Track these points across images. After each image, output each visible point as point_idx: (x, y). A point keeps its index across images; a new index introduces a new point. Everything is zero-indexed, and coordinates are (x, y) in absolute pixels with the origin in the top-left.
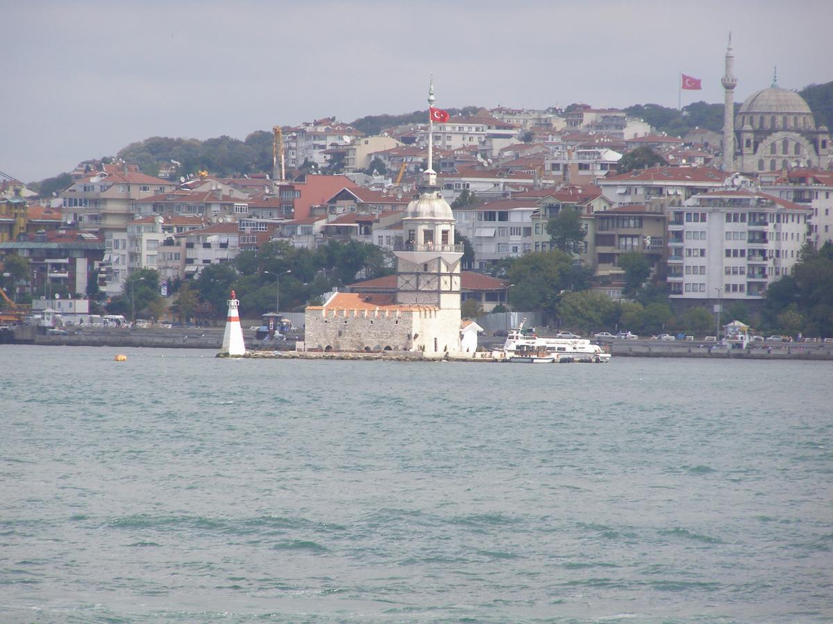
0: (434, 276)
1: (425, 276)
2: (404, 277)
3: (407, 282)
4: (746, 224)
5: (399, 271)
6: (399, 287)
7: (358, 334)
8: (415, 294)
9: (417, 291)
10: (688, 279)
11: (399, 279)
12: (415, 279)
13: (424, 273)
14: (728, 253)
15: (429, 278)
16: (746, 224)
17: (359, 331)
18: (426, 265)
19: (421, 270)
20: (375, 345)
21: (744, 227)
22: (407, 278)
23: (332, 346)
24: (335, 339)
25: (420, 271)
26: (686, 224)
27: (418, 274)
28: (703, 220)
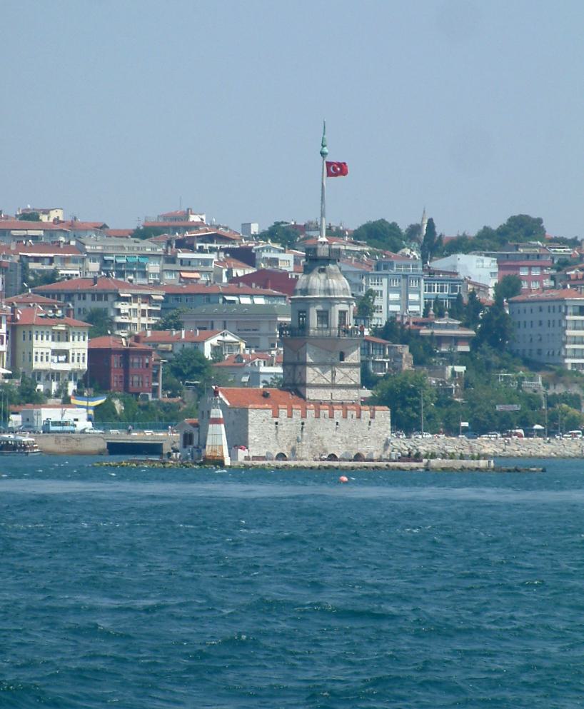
15: (346, 370)
17: (321, 435)
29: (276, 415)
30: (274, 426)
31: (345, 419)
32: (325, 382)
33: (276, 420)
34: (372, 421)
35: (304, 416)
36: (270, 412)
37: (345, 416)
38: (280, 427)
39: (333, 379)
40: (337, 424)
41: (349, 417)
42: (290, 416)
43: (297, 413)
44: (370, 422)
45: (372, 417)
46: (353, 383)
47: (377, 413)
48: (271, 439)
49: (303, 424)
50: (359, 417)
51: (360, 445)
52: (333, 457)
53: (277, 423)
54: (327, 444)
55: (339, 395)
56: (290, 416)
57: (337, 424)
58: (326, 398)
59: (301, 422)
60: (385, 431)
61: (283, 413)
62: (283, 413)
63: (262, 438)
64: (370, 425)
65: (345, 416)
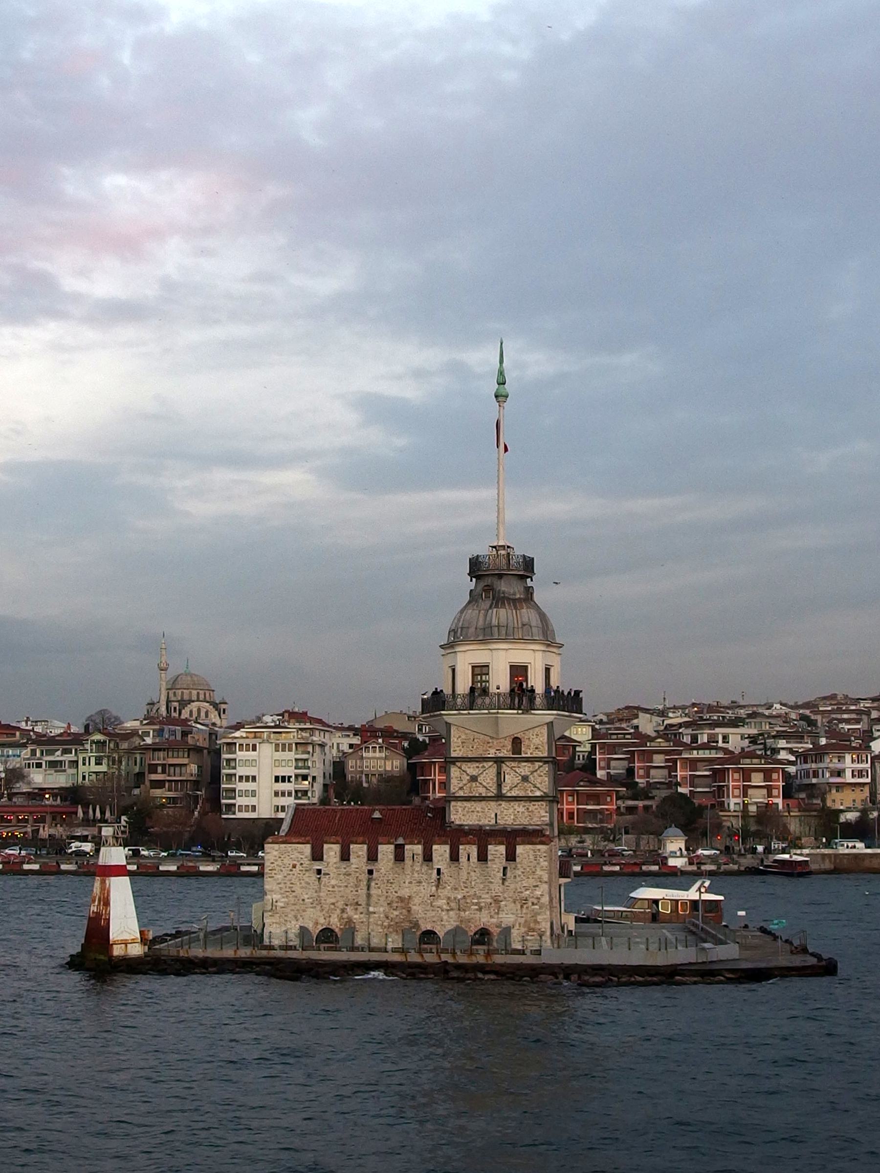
0: (537, 764)
1: (513, 764)
3: (474, 779)
4: (293, 753)
5: (453, 755)
6: (452, 790)
7: (401, 899)
9: (499, 797)
10: (240, 801)
11: (454, 771)
12: (493, 771)
13: (513, 760)
14: (277, 779)
15: (525, 769)
16: (293, 753)
17: (405, 892)
18: (517, 743)
20: (449, 928)
21: (291, 755)
22: (471, 769)
23: (337, 930)
24: (343, 911)
25: (505, 753)
26: (238, 752)
27: (499, 761)
28: (254, 749)
29: (317, 856)
30: (315, 877)
33: (317, 866)
35: (373, 857)
36: (307, 849)
37: (454, 857)
38: (324, 879)
39: (499, 786)
40: (439, 870)
41: (463, 859)
42: (345, 856)
43: (359, 851)
44: (505, 869)
45: (511, 856)
46: (538, 793)
47: (520, 849)
48: (307, 900)
49: (370, 872)
50: (483, 857)
51: (485, 912)
52: (429, 936)
53: (319, 872)
54: (417, 908)
55: (511, 815)
56: (345, 856)
57: (439, 870)
58: (484, 822)
59: (365, 869)
60: (537, 886)
61: (332, 851)
62: (332, 851)
63: (292, 900)
64: (504, 875)
65: (454, 857)
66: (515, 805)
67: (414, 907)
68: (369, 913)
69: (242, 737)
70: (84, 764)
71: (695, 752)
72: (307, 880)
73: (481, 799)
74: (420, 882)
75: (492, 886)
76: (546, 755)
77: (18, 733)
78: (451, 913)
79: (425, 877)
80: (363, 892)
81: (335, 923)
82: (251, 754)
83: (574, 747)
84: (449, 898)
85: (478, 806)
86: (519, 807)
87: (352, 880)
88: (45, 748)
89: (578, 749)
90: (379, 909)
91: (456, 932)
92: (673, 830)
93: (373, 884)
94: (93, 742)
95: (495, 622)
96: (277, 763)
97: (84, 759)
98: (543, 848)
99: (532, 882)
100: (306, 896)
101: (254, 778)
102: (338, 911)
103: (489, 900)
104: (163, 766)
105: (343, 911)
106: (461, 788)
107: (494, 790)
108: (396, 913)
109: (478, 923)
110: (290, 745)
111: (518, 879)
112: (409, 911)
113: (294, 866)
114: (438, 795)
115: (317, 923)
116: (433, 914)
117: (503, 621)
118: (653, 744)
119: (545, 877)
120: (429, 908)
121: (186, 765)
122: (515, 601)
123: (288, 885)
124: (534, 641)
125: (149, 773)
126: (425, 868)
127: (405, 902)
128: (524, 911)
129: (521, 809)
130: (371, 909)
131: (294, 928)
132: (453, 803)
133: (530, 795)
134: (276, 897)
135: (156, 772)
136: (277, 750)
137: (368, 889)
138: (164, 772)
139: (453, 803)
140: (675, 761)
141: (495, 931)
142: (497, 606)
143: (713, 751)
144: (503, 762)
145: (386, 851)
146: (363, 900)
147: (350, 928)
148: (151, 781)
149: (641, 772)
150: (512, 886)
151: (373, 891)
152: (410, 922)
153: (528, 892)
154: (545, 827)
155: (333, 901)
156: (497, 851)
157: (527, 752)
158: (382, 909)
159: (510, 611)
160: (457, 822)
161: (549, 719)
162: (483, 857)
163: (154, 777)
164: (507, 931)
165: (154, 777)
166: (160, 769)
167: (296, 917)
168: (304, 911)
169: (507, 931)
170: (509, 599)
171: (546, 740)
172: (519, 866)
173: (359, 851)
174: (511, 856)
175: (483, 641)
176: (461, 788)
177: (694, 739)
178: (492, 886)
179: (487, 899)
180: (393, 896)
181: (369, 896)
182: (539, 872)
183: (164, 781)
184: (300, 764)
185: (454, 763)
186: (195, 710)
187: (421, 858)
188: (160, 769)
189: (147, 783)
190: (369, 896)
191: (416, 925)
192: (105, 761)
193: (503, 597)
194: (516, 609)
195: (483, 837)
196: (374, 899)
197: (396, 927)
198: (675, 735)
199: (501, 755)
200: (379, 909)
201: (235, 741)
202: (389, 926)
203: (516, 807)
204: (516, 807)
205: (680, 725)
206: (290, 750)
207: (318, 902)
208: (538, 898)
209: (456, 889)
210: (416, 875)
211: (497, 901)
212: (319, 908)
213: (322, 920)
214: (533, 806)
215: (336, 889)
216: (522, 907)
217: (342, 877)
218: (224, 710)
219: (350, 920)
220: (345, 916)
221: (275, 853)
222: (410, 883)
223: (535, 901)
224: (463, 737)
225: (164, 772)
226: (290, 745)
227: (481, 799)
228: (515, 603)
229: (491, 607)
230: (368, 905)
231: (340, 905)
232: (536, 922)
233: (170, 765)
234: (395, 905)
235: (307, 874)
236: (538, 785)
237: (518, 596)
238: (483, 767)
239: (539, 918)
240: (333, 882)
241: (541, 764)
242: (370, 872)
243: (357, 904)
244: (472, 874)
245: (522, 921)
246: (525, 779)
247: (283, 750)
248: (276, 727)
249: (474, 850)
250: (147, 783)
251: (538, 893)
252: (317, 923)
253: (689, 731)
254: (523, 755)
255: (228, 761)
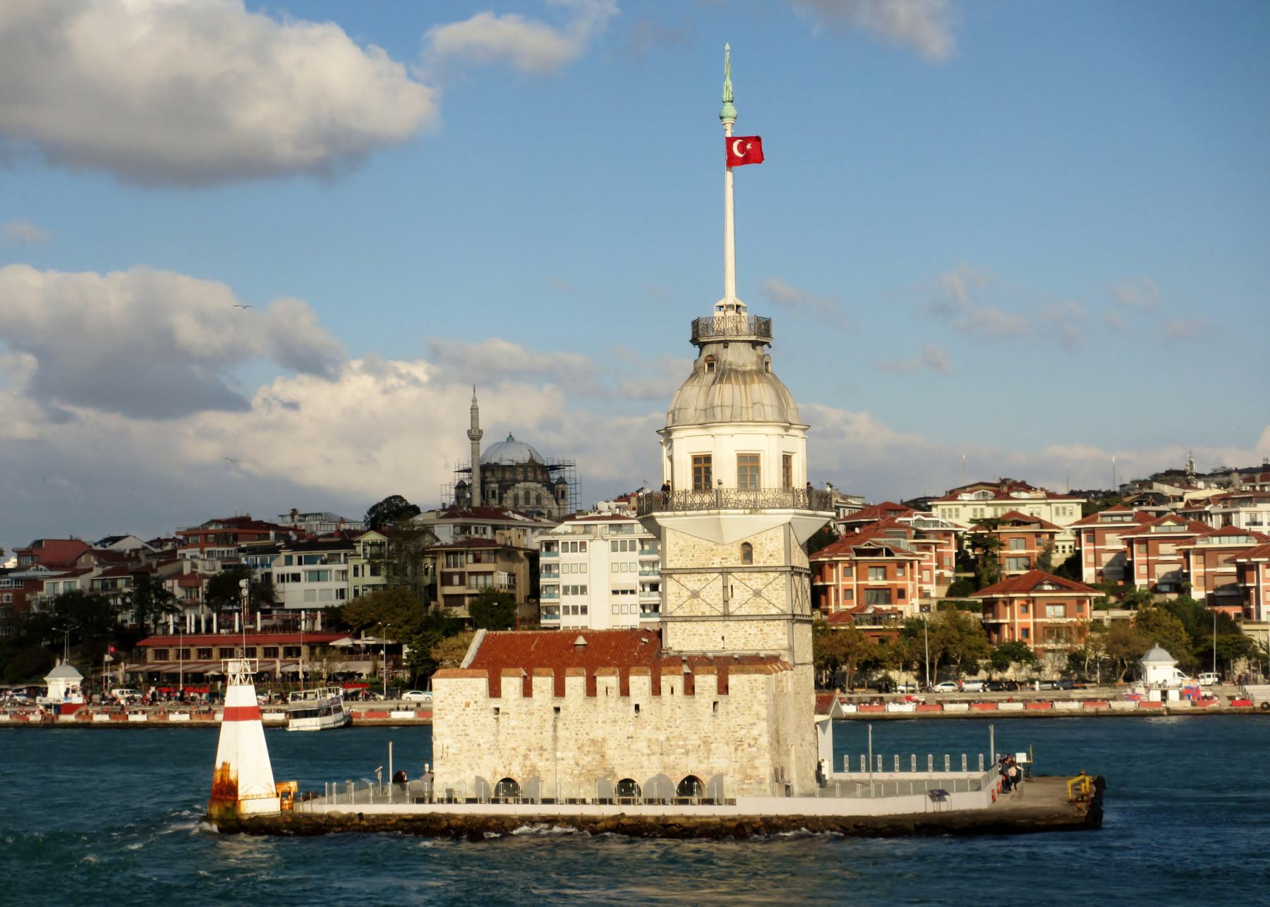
0: (772, 575)
1: (742, 575)
2: (683, 579)
3: (695, 595)
4: (637, 553)
8: (719, 625)
9: (727, 616)
11: (671, 586)
13: (742, 570)
15: (757, 581)
16: (637, 553)
17: (597, 734)
19: (735, 559)
21: (635, 556)
22: (692, 582)
23: (518, 780)
24: (526, 757)
27: (725, 572)
29: (495, 691)
30: (492, 716)
31: (657, 698)
32: (708, 611)
33: (495, 703)
34: (722, 699)
35: (559, 691)
36: (482, 683)
37: (656, 690)
40: (637, 707)
42: (527, 691)
43: (544, 684)
44: (715, 703)
45: (723, 688)
46: (774, 611)
47: (733, 680)
49: (557, 710)
50: (690, 689)
51: (693, 756)
52: (627, 788)
54: (612, 753)
55: (740, 639)
56: (527, 691)
57: (637, 707)
65: (656, 690)
66: (746, 626)
67: (609, 753)
68: (556, 759)
69: (566, 533)
70: (356, 574)
71: (1216, 539)
72: (482, 721)
73: (704, 618)
74: (615, 721)
75: (700, 725)
76: (782, 564)
77: (272, 534)
78: (653, 758)
79: (621, 715)
80: (549, 734)
81: (517, 774)
82: (577, 557)
83: (1052, 535)
84: (650, 740)
85: (701, 627)
86: (751, 628)
87: (535, 720)
88: (303, 554)
89: (1057, 537)
90: (568, 754)
91: (661, 779)
92: (1157, 652)
93: (560, 724)
94: (366, 544)
95: (717, 401)
96: (616, 568)
97: (356, 568)
98: (761, 678)
99: (749, 719)
100: (481, 741)
101: (584, 589)
102: (520, 758)
103: (698, 742)
104: (462, 575)
105: (526, 757)
106: (680, 607)
107: (720, 609)
108: (588, 759)
109: (684, 770)
110: (633, 542)
111: (731, 715)
112: (603, 756)
113: (468, 705)
114: (843, 607)
115: (495, 773)
116: (631, 759)
117: (728, 401)
118: (1159, 529)
119: (764, 713)
120: (626, 752)
121: (491, 573)
122: (744, 373)
123: (461, 727)
124: (765, 422)
125: (443, 584)
126: (621, 704)
127: (598, 745)
128: (739, 753)
129: (753, 631)
130: (559, 755)
131: (469, 778)
132: (670, 625)
133: (764, 613)
134: (447, 742)
135: (451, 584)
136: (614, 550)
137: (555, 731)
138: (462, 583)
139: (670, 625)
140: (1186, 554)
141: (705, 779)
142: (721, 381)
143: (1243, 539)
144: (730, 573)
145: (575, 683)
146: (548, 744)
147: (536, 780)
148: (445, 596)
149: (1144, 569)
150: (724, 724)
151: (560, 733)
152: (605, 769)
153: (743, 732)
154: (782, 652)
155: (515, 745)
156: (706, 682)
157: (759, 560)
158: (571, 755)
159: (736, 387)
160: (676, 648)
161: (787, 519)
162: (690, 689)
163: (449, 590)
164: (719, 778)
165: (449, 590)
166: (456, 579)
167: (470, 765)
168: (480, 758)
169: (719, 778)
170: (736, 372)
171: (782, 545)
172: (732, 700)
173: (544, 684)
174: (723, 688)
175: (703, 425)
176: (680, 607)
177: (1227, 517)
178: (700, 725)
179: (694, 740)
180: (583, 738)
181: (555, 739)
182: (756, 707)
183: (463, 596)
184: (647, 568)
185: (670, 575)
186: (521, 493)
187: (615, 691)
188: (456, 579)
189: (441, 600)
190: (555, 739)
191: (612, 773)
192: (383, 573)
193: (730, 370)
194: (745, 383)
195: (696, 663)
196: (561, 743)
197: (589, 776)
198: (1200, 515)
199: (728, 565)
200: (568, 754)
201: (556, 538)
202: (581, 774)
203: (747, 628)
204: (747, 628)
205: (1208, 501)
206: (633, 549)
207: (496, 747)
208: (756, 739)
209: (658, 729)
210: (610, 713)
211: (706, 742)
212: (496, 754)
213: (501, 769)
214: (768, 627)
215: (517, 731)
216: (736, 749)
217: (523, 716)
218: (563, 493)
219: (534, 769)
220: (528, 763)
221: (446, 690)
222: (604, 722)
223: (752, 742)
224: (682, 543)
225: (462, 583)
226: (633, 542)
227: (704, 618)
228: (742, 375)
229: (714, 383)
230: (555, 750)
231: (522, 750)
232: (753, 767)
233: (471, 574)
234: (586, 749)
235: (483, 714)
236: (774, 601)
237: (748, 368)
238: (706, 579)
239: (757, 763)
240: (513, 723)
241: (776, 575)
242: (557, 710)
243: (541, 748)
244: (677, 710)
245: (737, 766)
246: (757, 593)
247: (624, 549)
248: (614, 517)
249: (678, 682)
250: (441, 600)
251: (755, 732)
252: (495, 773)
253: (1220, 508)
254: (755, 564)
255: (549, 567)
